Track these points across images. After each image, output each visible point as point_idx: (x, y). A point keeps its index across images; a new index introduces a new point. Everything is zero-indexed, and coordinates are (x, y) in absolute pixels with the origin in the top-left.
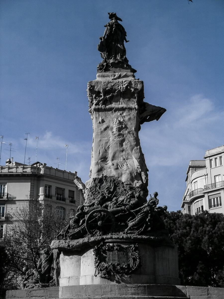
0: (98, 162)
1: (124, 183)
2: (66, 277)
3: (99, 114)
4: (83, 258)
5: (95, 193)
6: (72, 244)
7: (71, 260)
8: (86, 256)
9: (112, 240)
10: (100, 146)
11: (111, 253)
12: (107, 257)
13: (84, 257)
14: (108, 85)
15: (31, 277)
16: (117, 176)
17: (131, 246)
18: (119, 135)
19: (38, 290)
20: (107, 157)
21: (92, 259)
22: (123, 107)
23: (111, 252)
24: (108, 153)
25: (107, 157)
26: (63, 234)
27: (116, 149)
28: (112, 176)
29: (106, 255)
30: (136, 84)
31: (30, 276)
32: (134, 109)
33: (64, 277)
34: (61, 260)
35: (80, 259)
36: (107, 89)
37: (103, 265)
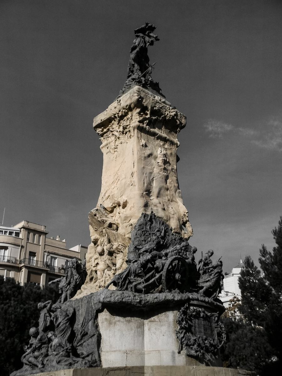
0: (143, 194)
1: (174, 229)
2: (120, 351)
3: (141, 135)
4: (149, 323)
5: (146, 233)
6: (146, 300)
7: (127, 323)
8: (157, 320)
9: (198, 302)
10: (143, 174)
11: (197, 321)
12: (192, 326)
13: (153, 321)
14: (156, 104)
15: (46, 346)
16: (166, 219)
17: (213, 314)
18: (165, 169)
19: (118, 370)
20: (151, 191)
21: (169, 326)
22: (166, 138)
23: (197, 319)
24: (152, 187)
25: (151, 191)
26: (119, 283)
27: (162, 185)
28: (160, 216)
29: (192, 322)
30: (181, 117)
31: (44, 343)
32: (175, 145)
33: (113, 350)
34: (103, 322)
35: (143, 324)
36: (155, 108)
37: (188, 337)
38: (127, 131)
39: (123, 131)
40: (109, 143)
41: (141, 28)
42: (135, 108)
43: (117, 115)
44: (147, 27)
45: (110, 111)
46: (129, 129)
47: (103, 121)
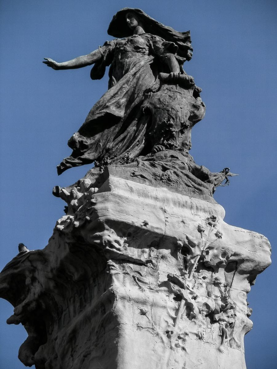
38: (224, 321)
39: (216, 310)
40: (154, 305)
41: (166, 27)
42: (246, 276)
43: (197, 251)
44: (181, 43)
45: (178, 222)
46: (231, 320)
47: (147, 231)
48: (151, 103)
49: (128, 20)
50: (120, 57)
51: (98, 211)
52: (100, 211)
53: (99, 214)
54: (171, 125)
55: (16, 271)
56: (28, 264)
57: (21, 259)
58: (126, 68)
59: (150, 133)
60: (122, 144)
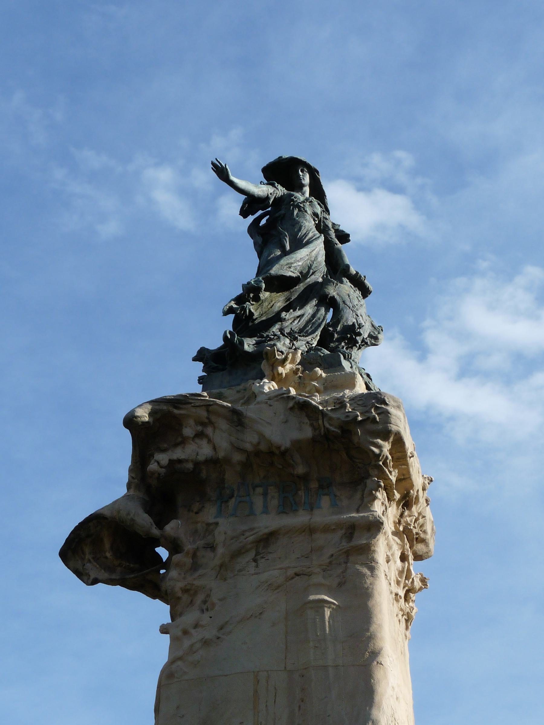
48: (338, 294)
49: (301, 173)
50: (296, 212)
51: (393, 416)
52: (394, 417)
53: (393, 421)
54: (359, 334)
55: (176, 411)
56: (203, 413)
57: (193, 401)
58: (303, 231)
59: (330, 329)
60: (299, 321)
